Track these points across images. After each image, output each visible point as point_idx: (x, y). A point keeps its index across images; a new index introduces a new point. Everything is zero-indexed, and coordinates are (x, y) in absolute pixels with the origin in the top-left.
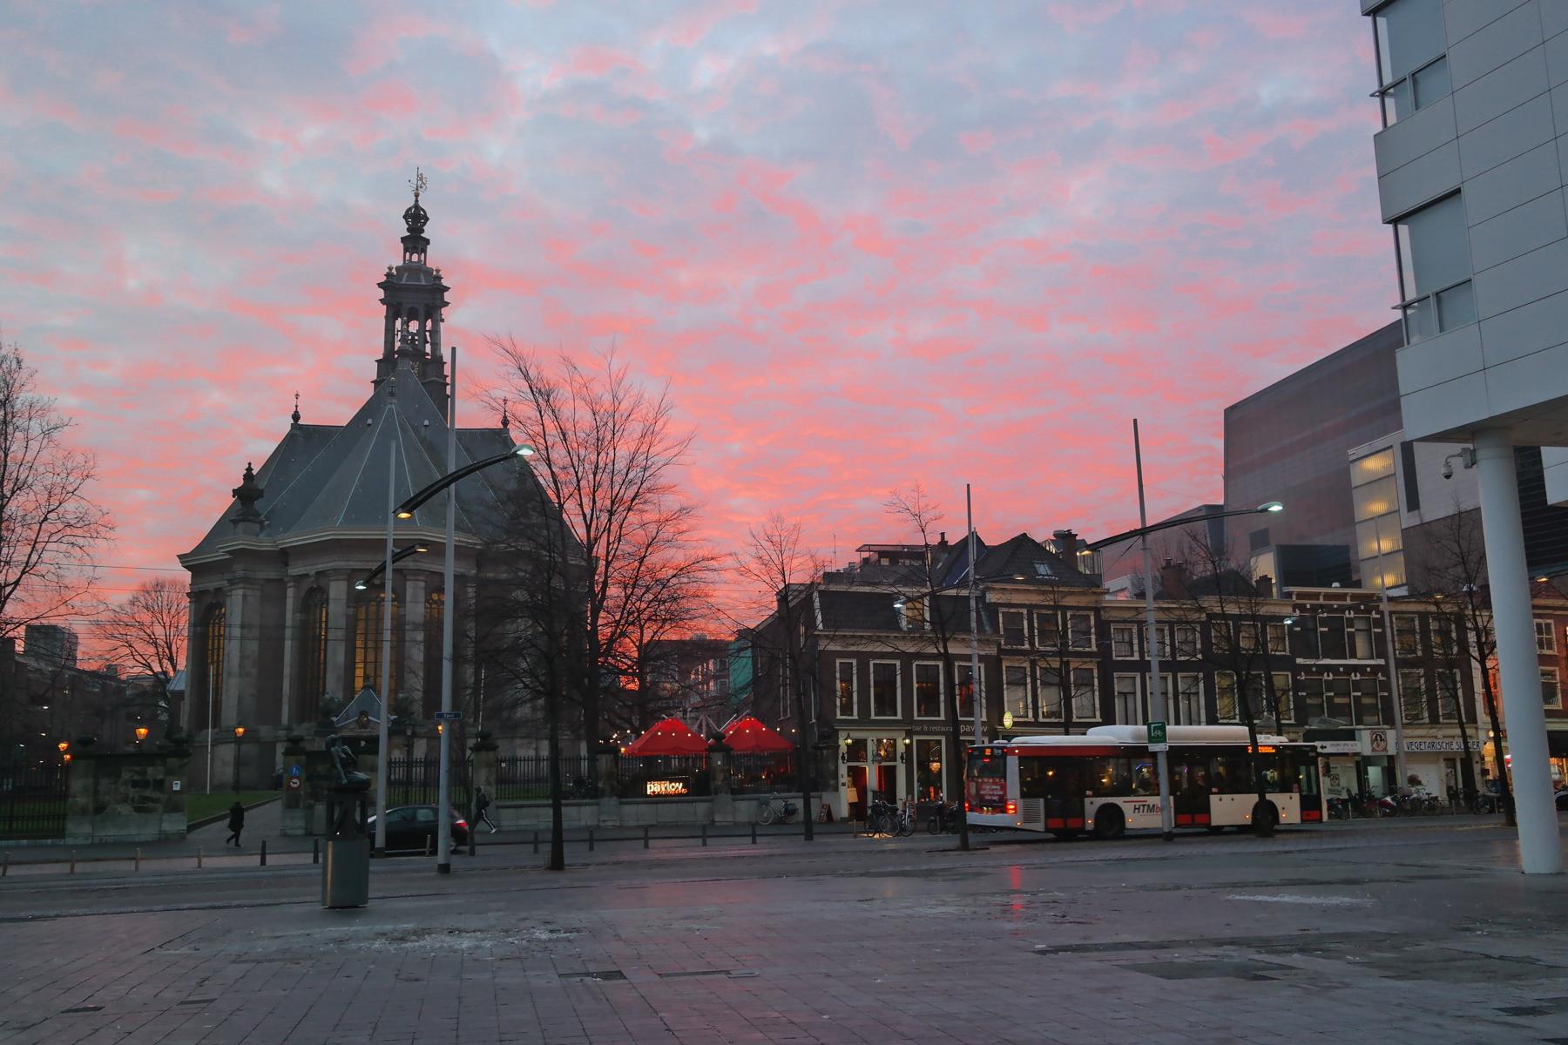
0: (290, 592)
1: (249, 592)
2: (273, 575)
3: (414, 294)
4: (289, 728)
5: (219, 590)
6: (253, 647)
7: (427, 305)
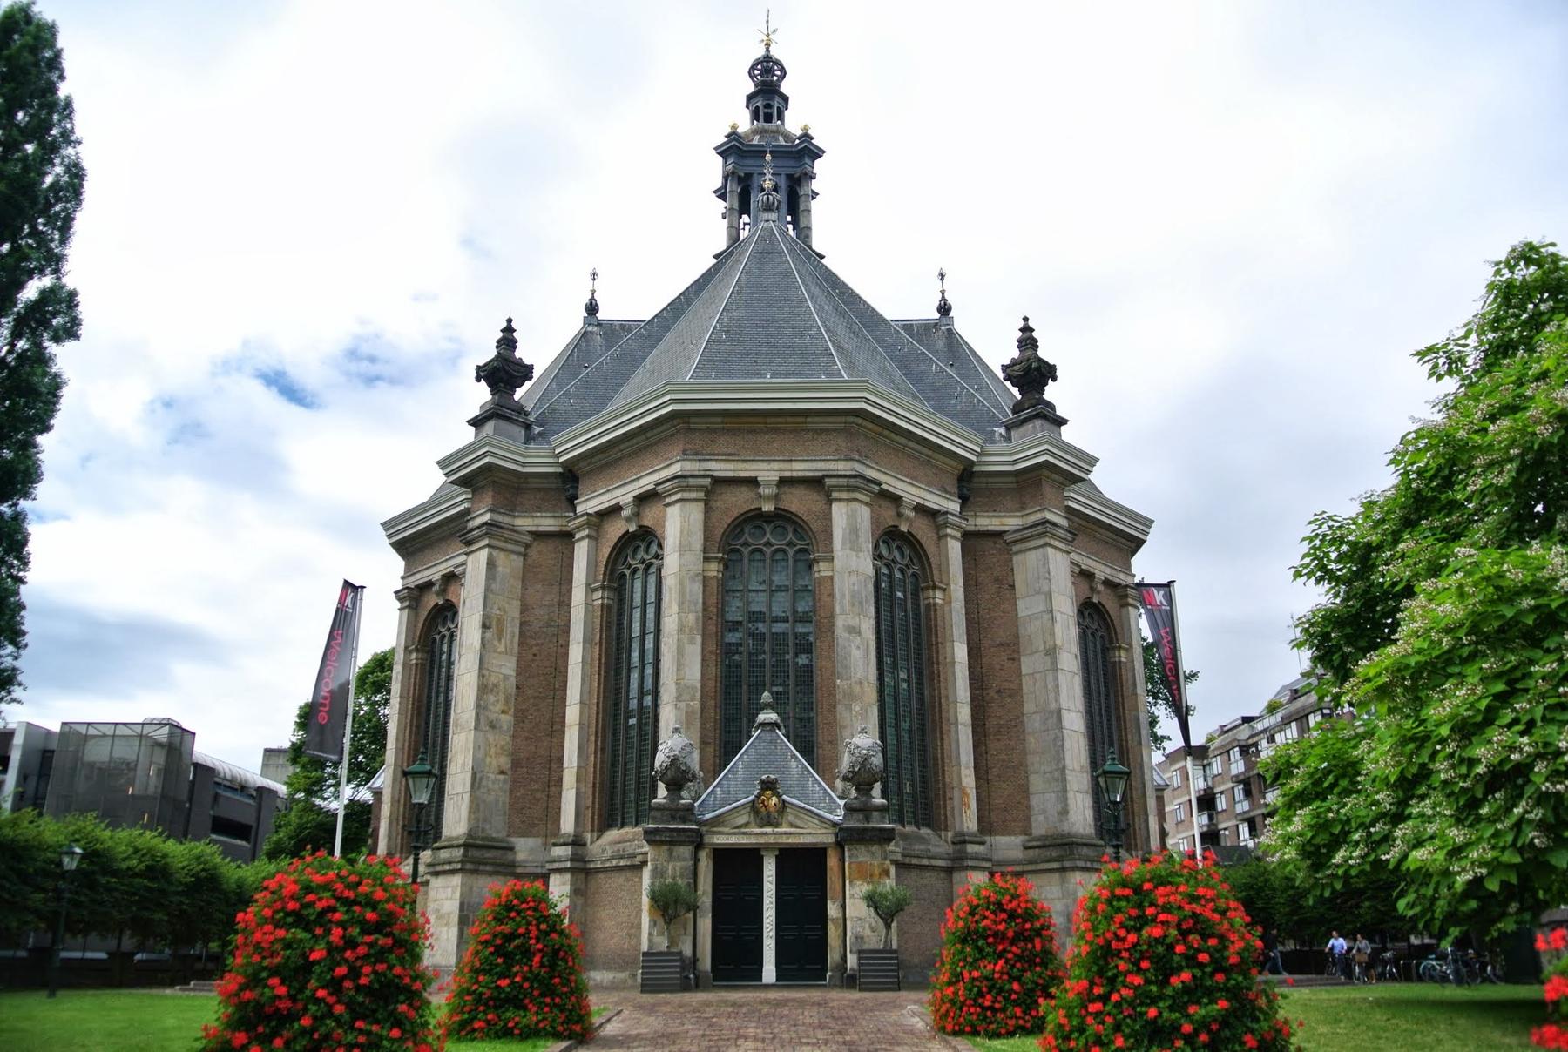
0: (581, 551)
1: (501, 558)
2: (548, 524)
3: (768, 169)
4: (577, 842)
5: (451, 578)
6: (506, 667)
7: (790, 177)
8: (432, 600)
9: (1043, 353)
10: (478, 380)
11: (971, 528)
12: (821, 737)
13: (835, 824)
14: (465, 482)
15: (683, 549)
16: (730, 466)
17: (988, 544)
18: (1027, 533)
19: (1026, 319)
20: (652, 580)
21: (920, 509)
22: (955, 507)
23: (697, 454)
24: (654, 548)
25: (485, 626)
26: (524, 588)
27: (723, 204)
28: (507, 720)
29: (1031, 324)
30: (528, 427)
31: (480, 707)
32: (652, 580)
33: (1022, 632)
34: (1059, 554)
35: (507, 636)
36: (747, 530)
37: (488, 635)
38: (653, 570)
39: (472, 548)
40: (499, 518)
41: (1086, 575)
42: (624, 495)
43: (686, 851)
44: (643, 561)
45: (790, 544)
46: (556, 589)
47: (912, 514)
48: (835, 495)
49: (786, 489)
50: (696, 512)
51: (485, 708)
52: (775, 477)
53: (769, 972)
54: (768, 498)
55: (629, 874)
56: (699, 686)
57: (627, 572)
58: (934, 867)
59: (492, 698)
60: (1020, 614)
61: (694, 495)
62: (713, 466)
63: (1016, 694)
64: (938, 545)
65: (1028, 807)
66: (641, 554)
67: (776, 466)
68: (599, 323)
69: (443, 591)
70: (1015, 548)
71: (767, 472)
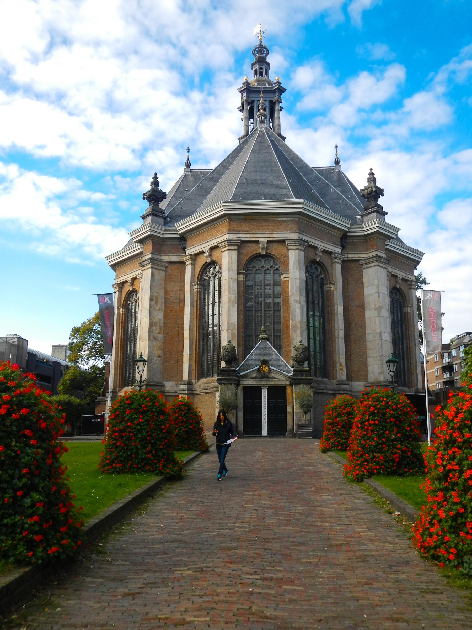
0: (188, 269)
1: (156, 272)
2: (174, 258)
4: (189, 383)
5: (134, 279)
8: (128, 288)
9: (378, 184)
10: (144, 199)
11: (346, 259)
12: (283, 344)
13: (290, 377)
14: (141, 241)
15: (229, 269)
16: (248, 236)
17: (353, 264)
18: (369, 260)
19: (371, 169)
20: (217, 281)
21: (325, 252)
22: (339, 250)
23: (234, 231)
24: (217, 268)
25: (151, 300)
26: (166, 284)
27: (241, 114)
28: (160, 336)
29: (373, 171)
30: (165, 219)
31: (150, 331)
32: (217, 281)
33: (366, 301)
34: (382, 269)
35: (160, 303)
36: (254, 261)
37: (152, 303)
38: (217, 277)
39: (144, 268)
40: (155, 256)
41: (395, 276)
42: (205, 247)
43: (233, 387)
44: (213, 274)
45: (272, 267)
46: (178, 284)
47: (321, 254)
48: (290, 247)
49: (270, 245)
50: (234, 255)
51: (152, 332)
52: (266, 240)
53: (265, 432)
54: (263, 249)
55: (210, 395)
56: (236, 323)
57: (207, 278)
58: (328, 394)
59: (154, 328)
60: (365, 294)
61: (233, 248)
62: (240, 236)
63: (363, 326)
64: (332, 266)
65: (367, 371)
66: (212, 271)
67: (266, 235)
68: (191, 171)
69: (132, 284)
70: (364, 267)
71: (263, 238)
